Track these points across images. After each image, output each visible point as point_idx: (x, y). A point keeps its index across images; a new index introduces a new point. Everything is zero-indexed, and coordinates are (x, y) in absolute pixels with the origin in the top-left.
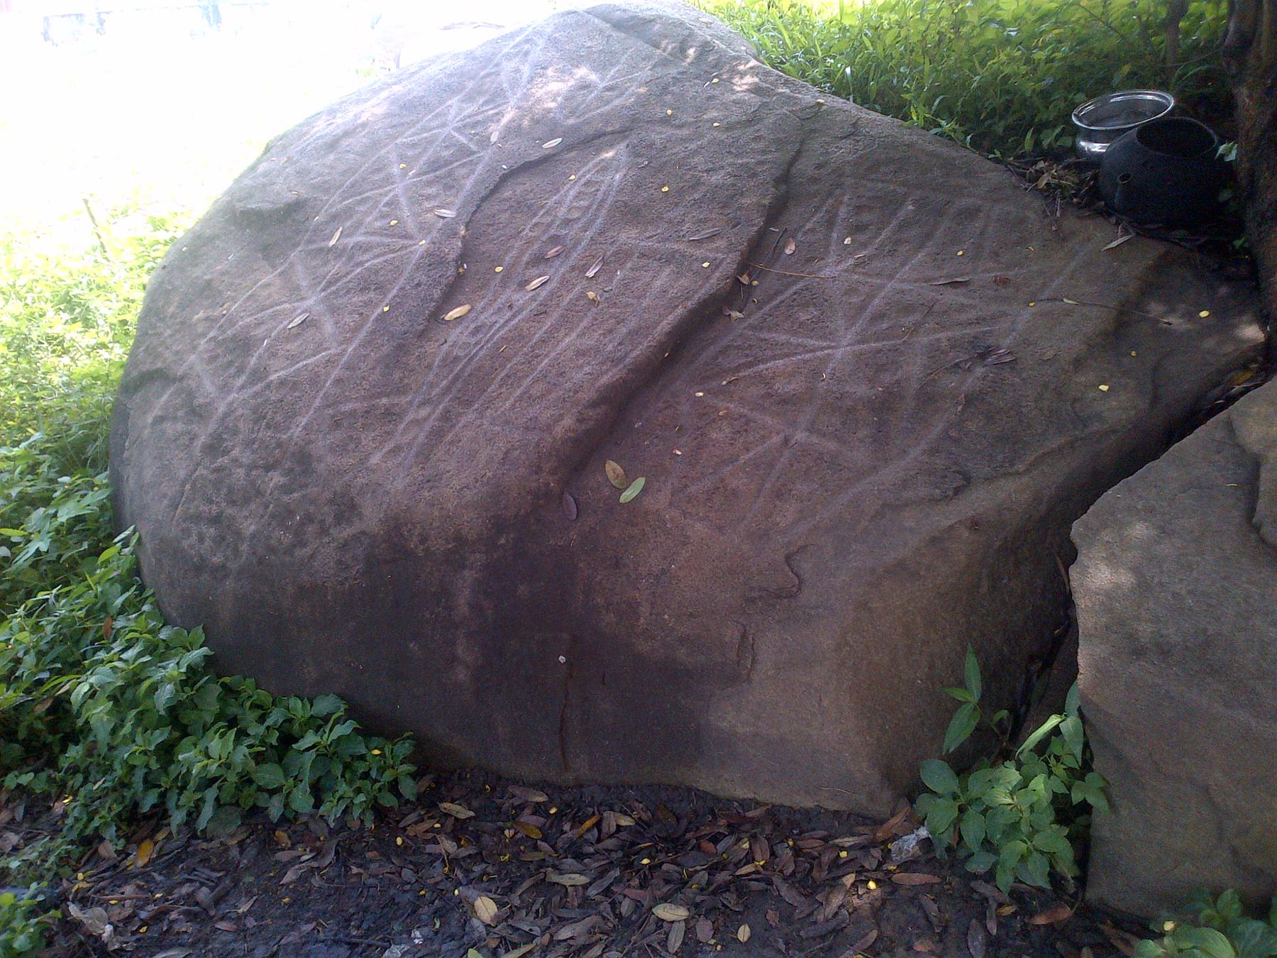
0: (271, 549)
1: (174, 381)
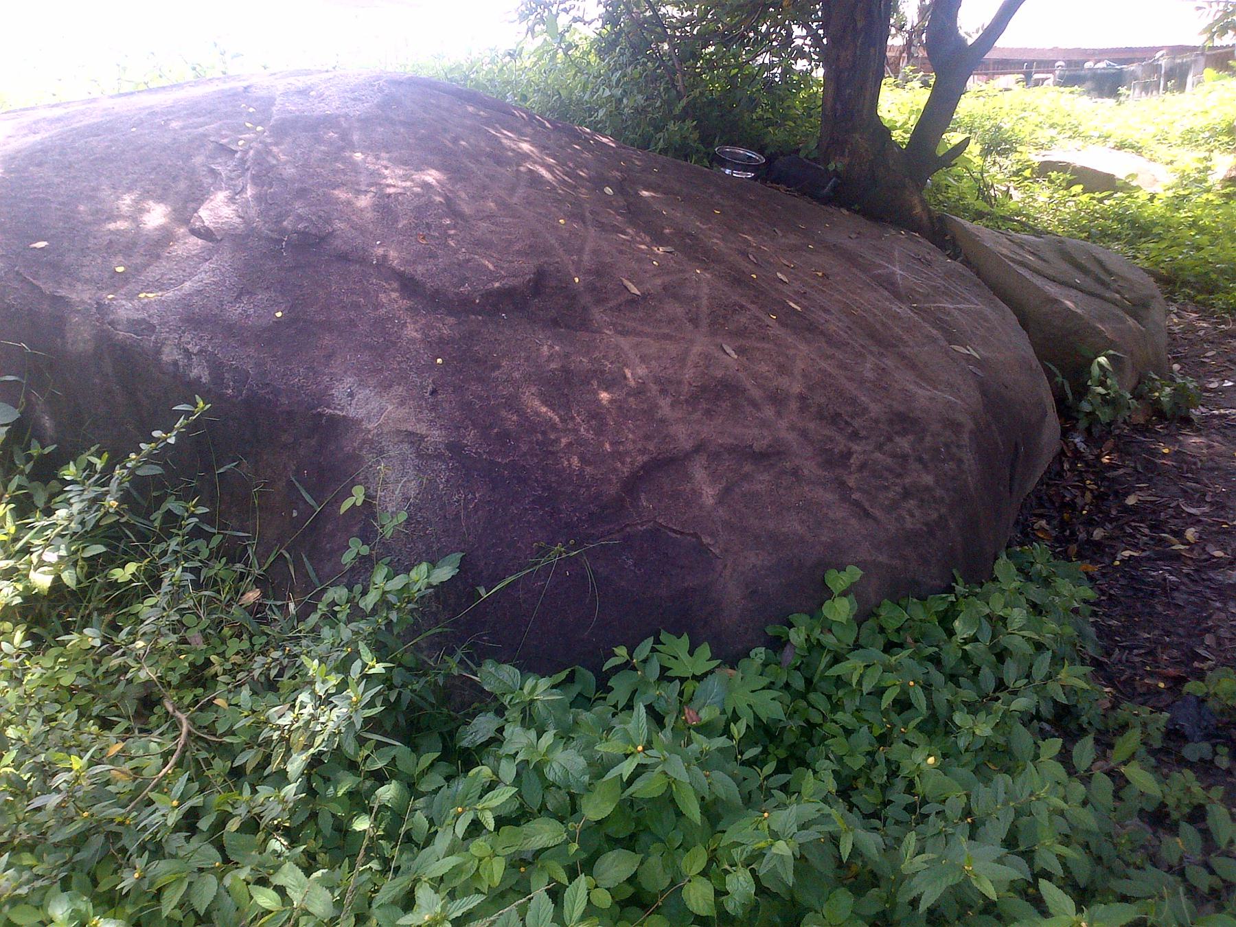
1: (688, 456)
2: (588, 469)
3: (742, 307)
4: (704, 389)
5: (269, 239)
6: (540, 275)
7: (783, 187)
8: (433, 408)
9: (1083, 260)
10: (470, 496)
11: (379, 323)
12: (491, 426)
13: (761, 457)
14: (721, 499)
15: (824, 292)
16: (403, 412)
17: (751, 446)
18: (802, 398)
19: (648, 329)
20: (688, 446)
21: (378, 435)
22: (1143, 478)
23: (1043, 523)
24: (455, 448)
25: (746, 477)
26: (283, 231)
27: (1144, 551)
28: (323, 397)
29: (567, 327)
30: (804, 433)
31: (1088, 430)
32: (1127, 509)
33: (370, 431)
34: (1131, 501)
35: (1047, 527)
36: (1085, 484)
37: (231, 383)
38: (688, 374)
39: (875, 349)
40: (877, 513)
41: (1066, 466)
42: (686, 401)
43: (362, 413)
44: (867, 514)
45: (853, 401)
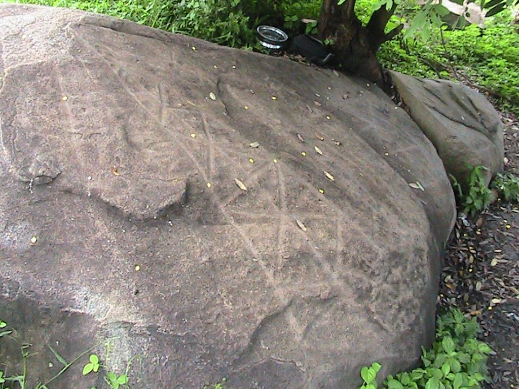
0: (422, 289)
1: (285, 309)
2: (231, 331)
3: (303, 187)
4: (290, 259)
5: (20, 181)
6: (188, 186)
7: (299, 57)
8: (137, 304)
9: (462, 99)
10: (162, 358)
11: (98, 242)
12: (173, 311)
13: (325, 302)
14: (305, 337)
15: (342, 158)
16: (120, 308)
17: (319, 296)
18: (344, 254)
19: (253, 216)
20: (285, 302)
21: (105, 325)
22: (498, 245)
23: (449, 277)
24: (152, 329)
25: (318, 317)
26: (30, 176)
27: (503, 299)
28: (69, 301)
29: (207, 223)
30: (346, 279)
31: (469, 213)
32: (491, 269)
33: (100, 323)
34: (494, 263)
35: (452, 280)
36: (469, 249)
37: (8, 290)
38: (281, 249)
39: (374, 202)
40: (386, 326)
41: (458, 235)
42: (282, 270)
43: (93, 312)
44: (382, 328)
45: (370, 250)
